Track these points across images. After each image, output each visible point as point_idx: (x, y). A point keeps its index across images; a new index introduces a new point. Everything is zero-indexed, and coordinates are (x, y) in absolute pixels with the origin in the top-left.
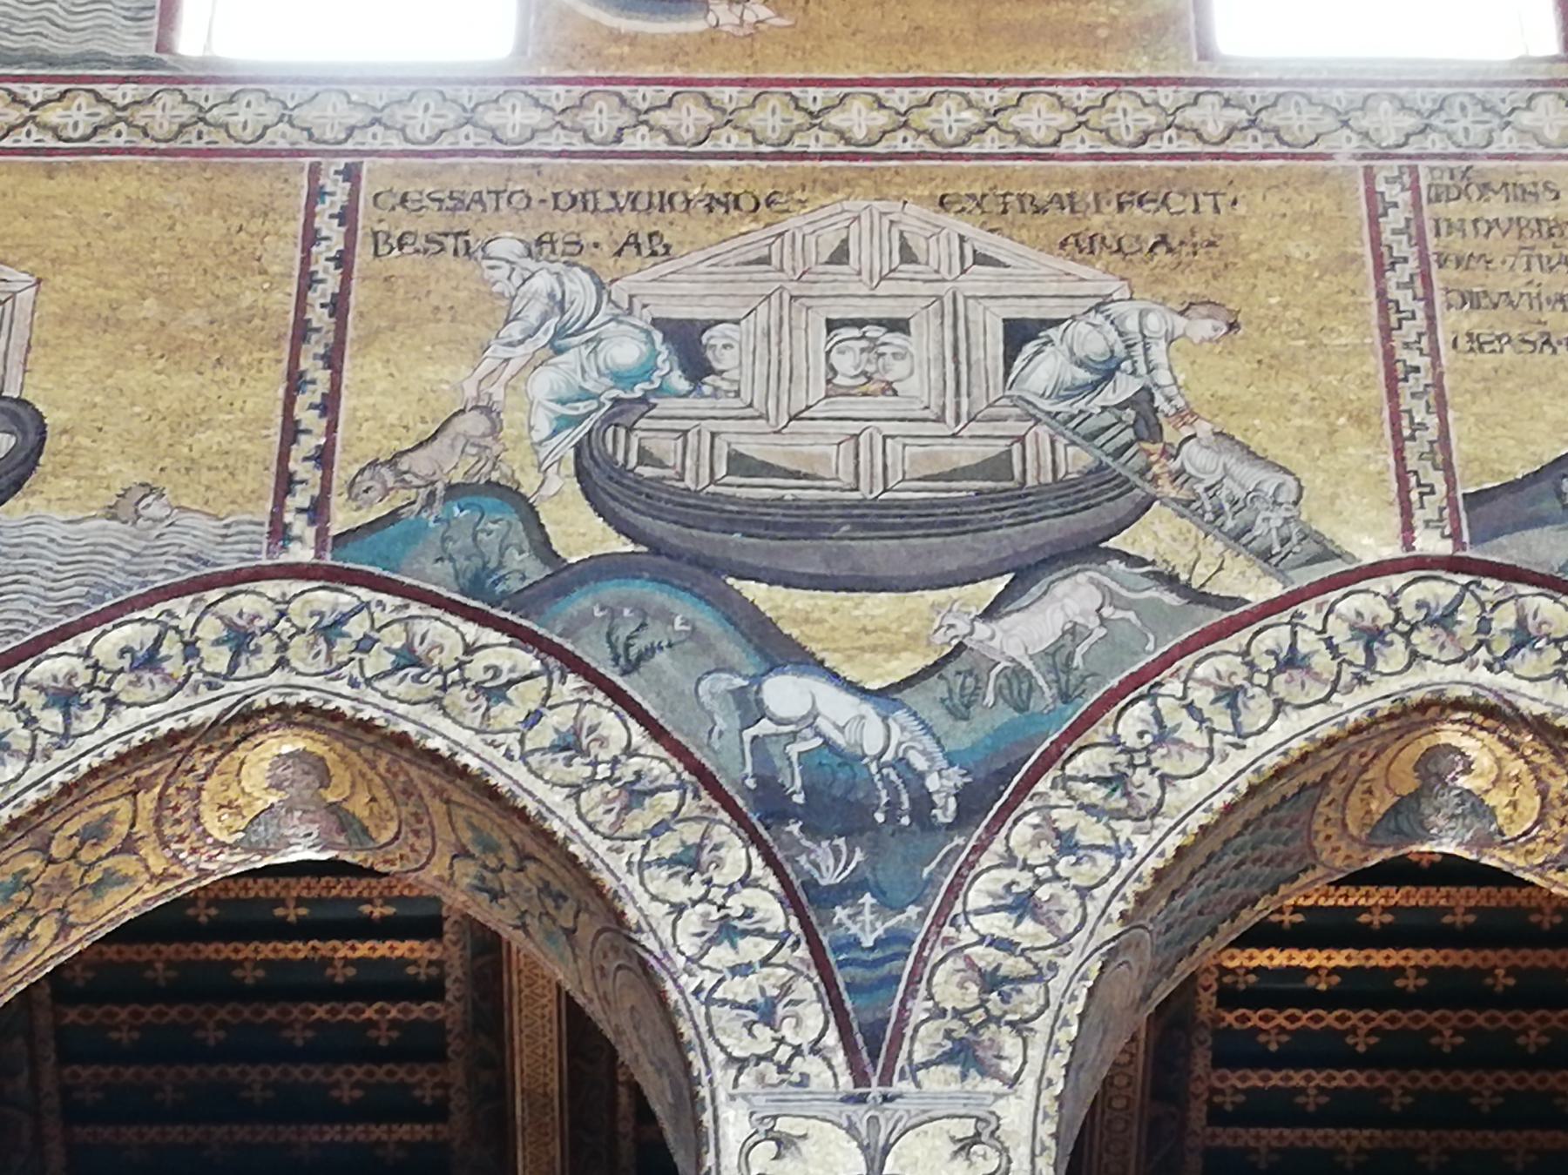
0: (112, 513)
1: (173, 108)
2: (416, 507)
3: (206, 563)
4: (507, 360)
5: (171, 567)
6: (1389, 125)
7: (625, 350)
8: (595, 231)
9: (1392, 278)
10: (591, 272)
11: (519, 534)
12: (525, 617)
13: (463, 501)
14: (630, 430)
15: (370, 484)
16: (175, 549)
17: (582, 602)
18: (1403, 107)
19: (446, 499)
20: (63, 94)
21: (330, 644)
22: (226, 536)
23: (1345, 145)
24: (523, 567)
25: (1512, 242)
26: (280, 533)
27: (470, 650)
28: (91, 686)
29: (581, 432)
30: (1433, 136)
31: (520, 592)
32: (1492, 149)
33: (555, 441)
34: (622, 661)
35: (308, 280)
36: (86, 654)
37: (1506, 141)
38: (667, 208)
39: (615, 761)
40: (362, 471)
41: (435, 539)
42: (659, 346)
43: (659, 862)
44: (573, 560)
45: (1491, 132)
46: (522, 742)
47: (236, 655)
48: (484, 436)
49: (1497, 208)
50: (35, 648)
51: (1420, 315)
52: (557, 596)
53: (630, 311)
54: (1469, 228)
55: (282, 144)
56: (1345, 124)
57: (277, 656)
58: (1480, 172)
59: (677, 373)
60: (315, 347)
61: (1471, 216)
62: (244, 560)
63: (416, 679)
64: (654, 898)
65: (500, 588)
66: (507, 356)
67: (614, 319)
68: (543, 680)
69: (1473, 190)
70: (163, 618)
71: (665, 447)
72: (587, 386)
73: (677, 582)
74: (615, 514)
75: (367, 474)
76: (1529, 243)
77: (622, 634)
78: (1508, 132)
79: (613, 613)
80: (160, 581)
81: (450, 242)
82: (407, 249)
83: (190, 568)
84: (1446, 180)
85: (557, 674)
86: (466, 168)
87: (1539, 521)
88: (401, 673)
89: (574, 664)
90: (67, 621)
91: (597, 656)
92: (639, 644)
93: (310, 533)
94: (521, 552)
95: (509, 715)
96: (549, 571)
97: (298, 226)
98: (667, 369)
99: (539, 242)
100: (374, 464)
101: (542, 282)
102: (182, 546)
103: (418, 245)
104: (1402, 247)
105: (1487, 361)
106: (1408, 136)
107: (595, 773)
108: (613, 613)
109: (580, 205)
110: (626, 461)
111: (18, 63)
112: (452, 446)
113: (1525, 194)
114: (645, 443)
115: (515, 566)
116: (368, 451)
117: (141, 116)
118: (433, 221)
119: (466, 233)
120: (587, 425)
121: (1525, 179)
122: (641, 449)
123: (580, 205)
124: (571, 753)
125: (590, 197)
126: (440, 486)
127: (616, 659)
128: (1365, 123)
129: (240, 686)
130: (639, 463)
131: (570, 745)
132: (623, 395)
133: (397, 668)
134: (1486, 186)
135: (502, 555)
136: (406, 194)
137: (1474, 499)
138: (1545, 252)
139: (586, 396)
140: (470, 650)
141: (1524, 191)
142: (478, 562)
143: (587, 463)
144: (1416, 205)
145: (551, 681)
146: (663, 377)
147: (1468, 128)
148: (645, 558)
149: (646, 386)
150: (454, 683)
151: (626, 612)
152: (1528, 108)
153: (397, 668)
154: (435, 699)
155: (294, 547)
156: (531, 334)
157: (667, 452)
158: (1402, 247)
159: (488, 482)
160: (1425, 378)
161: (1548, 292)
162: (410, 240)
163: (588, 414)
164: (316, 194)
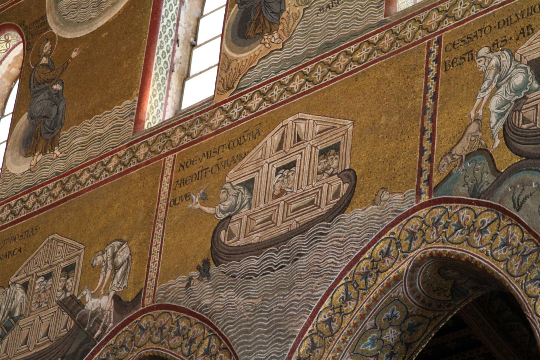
0: (374, 203)
1: (390, 37)
2: (457, 168)
3: (400, 212)
4: (483, 98)
5: (390, 217)
7: (518, 80)
8: (510, 32)
10: (508, 51)
11: (487, 168)
12: (488, 199)
13: (470, 161)
14: (520, 111)
15: (443, 164)
16: (390, 210)
17: (506, 187)
19: (466, 160)
21: (437, 228)
22: (404, 200)
24: (489, 178)
26: (419, 193)
27: (476, 216)
28: (373, 269)
29: (504, 119)
31: (487, 189)
33: (497, 125)
34: (517, 206)
35: (427, 89)
36: (370, 257)
38: (533, 13)
39: (519, 245)
40: (442, 159)
41: (461, 178)
42: (530, 73)
43: (532, 281)
44: (503, 171)
46: (491, 248)
47: (411, 242)
48: (476, 132)
50: (357, 259)
52: (498, 187)
53: (521, 62)
55: (420, 38)
57: (422, 239)
59: (534, 82)
60: (428, 116)
62: (409, 207)
63: (462, 234)
64: (529, 296)
65: (482, 190)
66: (483, 96)
67: (516, 67)
68: (498, 222)
70: (391, 236)
71: (530, 114)
72: (507, 98)
73: (533, 168)
74: (515, 148)
75: (443, 160)
77: (516, 195)
79: (514, 187)
80: (387, 223)
81: (467, 57)
82: (455, 65)
83: (395, 215)
85: (501, 218)
86: (472, 24)
88: (456, 233)
89: (505, 212)
90: (363, 247)
91: (509, 206)
92: (521, 198)
93: (427, 191)
94: (487, 173)
95: (487, 237)
96: (495, 178)
97: (424, 69)
98: (531, 81)
99: (494, 45)
100: (444, 156)
101: (494, 62)
102: (392, 208)
103: (458, 62)
107: (513, 252)
108: (514, 187)
109: (506, 23)
110: (518, 125)
111: (348, 39)
112: (467, 139)
114: (525, 115)
115: (486, 180)
116: (442, 151)
117: (380, 45)
118: (463, 49)
119: (472, 51)
120: (507, 113)
122: (523, 117)
123: (506, 23)
124: (505, 247)
125: (509, 19)
126: (464, 157)
127: (515, 207)
129: (412, 254)
130: (523, 124)
131: (505, 244)
132: (518, 97)
133: (456, 231)
135: (482, 177)
136: (454, 42)
139: (508, 102)
140: (476, 216)
142: (475, 182)
143: (507, 130)
145: (500, 220)
146: (530, 85)
148: (524, 162)
149: (525, 91)
150: (472, 231)
151: (518, 186)
153: (456, 231)
154: (377, 273)
155: (423, 196)
156: (490, 84)
157: (531, 116)
159: (478, 150)
162: (455, 61)
163: (507, 111)
164: (429, 53)
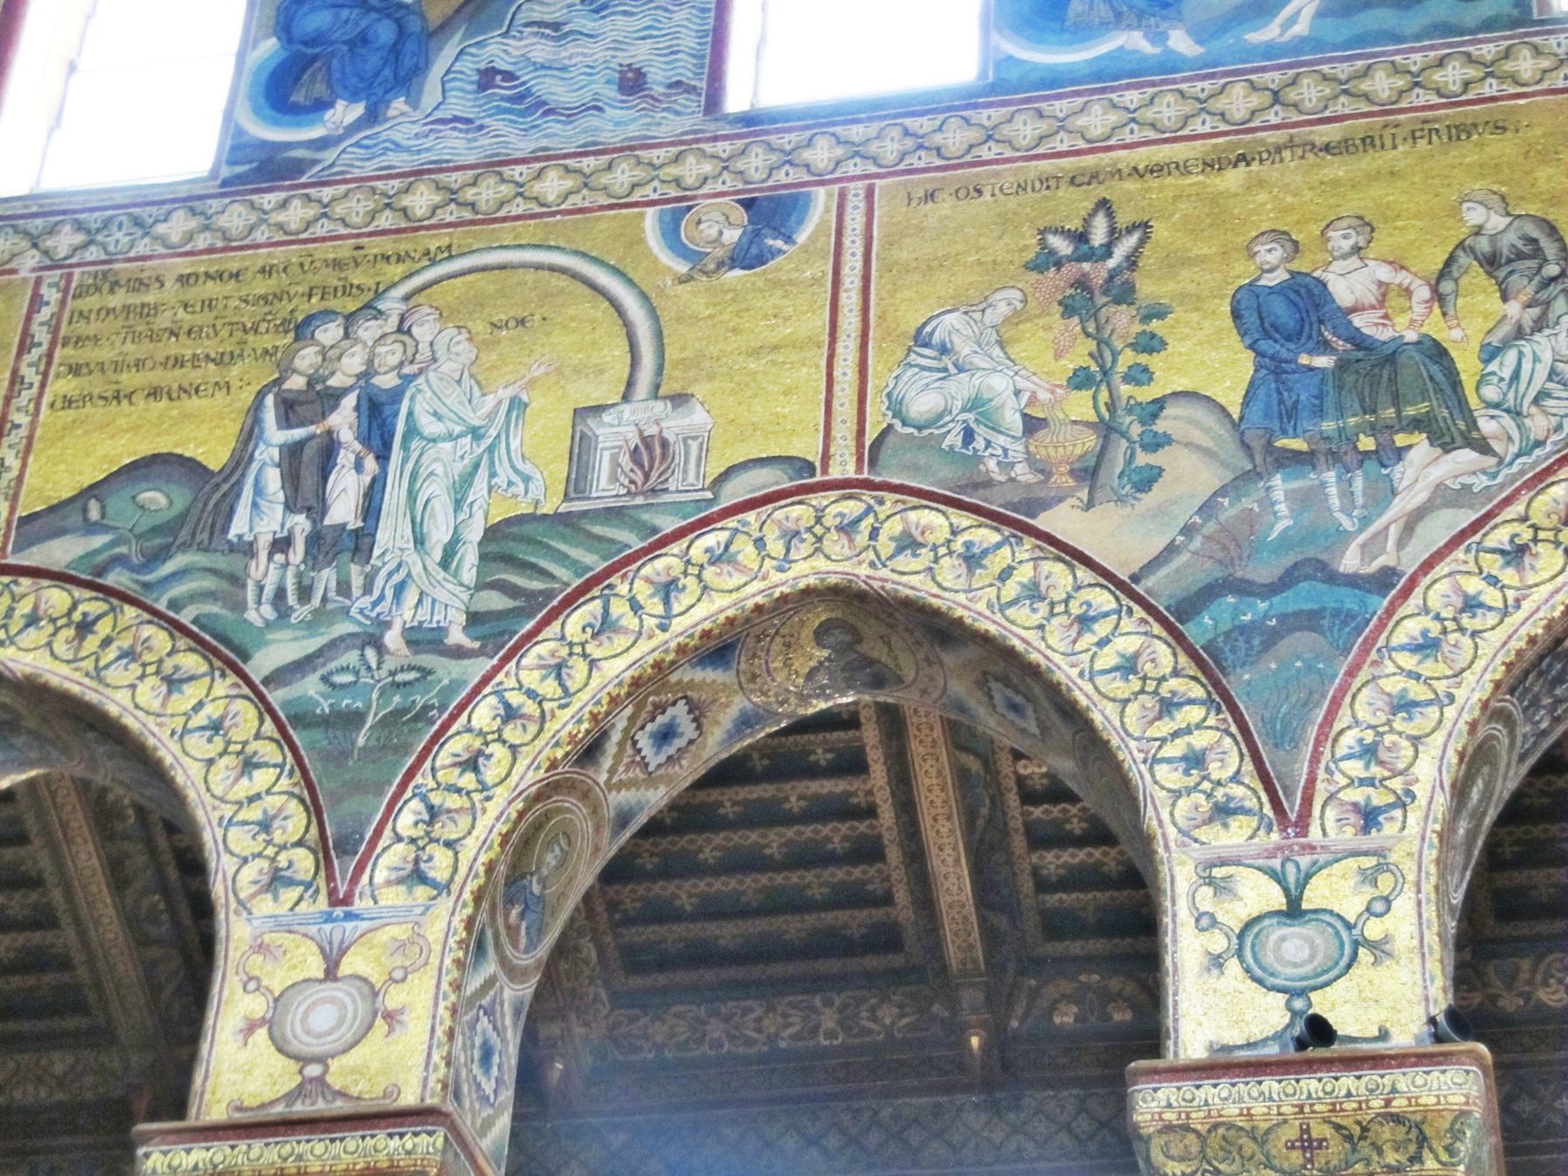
6: (64, 242)
9: (27, 358)
18: (79, 227)
20: (346, 195)
23: (31, 259)
25: (120, 322)
30: (93, 248)
32: (132, 254)
37: (142, 248)
45: (133, 241)
49: (118, 299)
51: (36, 385)
54: (93, 316)
56: (35, 246)
58: (116, 273)
61: (97, 306)
69: (106, 287)
76: (131, 322)
78: (147, 240)
84: (91, 281)
87: (60, 532)
104: (41, 335)
105: (71, 414)
106: (75, 250)
113: (139, 285)
121: (143, 275)
128: (49, 243)
134: (116, 283)
137: (24, 521)
138: (139, 329)
141: (141, 283)
144: (63, 303)
147: (118, 238)
152: (165, 220)
158: (41, 335)
160: (23, 432)
161: (131, 359)
